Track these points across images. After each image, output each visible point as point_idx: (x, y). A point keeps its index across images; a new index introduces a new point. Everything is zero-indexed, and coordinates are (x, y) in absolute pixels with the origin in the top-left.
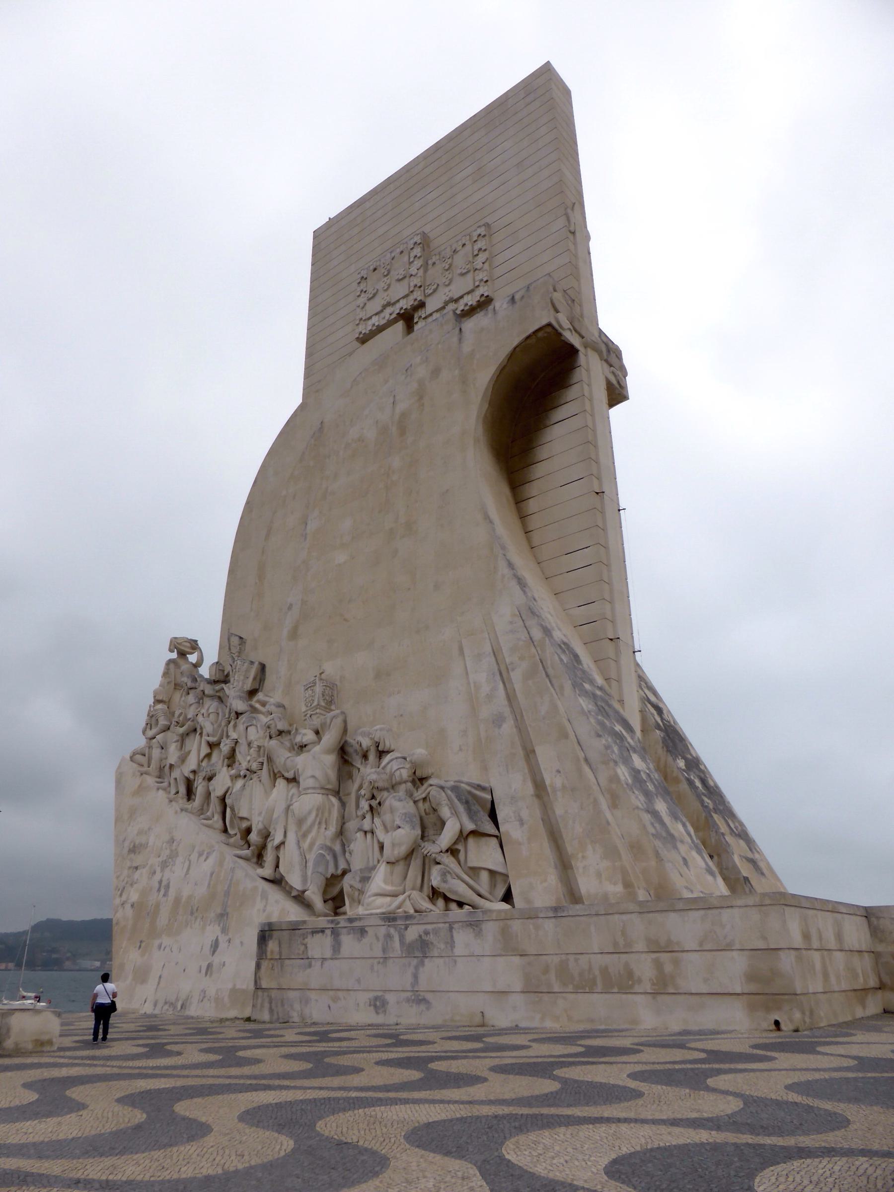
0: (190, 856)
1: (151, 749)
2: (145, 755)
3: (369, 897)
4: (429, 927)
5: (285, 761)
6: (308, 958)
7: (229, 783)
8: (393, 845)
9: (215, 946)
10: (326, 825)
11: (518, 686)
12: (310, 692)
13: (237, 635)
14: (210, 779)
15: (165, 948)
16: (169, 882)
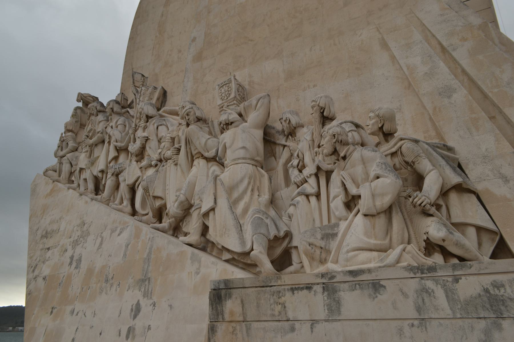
0: (102, 233)
1: (61, 164)
2: (56, 172)
3: (348, 252)
4: (499, 278)
5: (206, 141)
6: (288, 321)
7: (138, 173)
8: (373, 196)
9: (137, 310)
10: (259, 192)
11: (465, 63)
12: (227, 88)
13: (140, 73)
14: (117, 175)
15: (78, 313)
16: (81, 257)
